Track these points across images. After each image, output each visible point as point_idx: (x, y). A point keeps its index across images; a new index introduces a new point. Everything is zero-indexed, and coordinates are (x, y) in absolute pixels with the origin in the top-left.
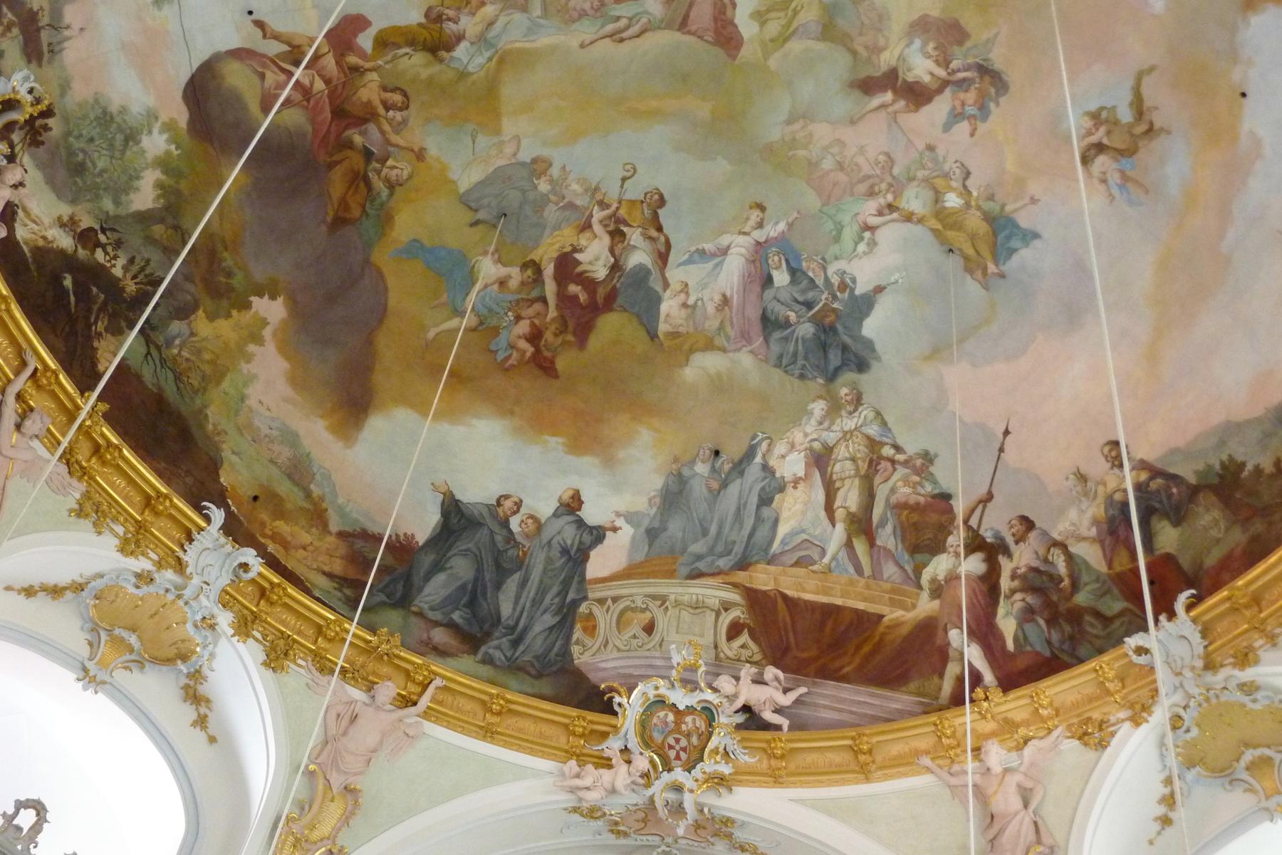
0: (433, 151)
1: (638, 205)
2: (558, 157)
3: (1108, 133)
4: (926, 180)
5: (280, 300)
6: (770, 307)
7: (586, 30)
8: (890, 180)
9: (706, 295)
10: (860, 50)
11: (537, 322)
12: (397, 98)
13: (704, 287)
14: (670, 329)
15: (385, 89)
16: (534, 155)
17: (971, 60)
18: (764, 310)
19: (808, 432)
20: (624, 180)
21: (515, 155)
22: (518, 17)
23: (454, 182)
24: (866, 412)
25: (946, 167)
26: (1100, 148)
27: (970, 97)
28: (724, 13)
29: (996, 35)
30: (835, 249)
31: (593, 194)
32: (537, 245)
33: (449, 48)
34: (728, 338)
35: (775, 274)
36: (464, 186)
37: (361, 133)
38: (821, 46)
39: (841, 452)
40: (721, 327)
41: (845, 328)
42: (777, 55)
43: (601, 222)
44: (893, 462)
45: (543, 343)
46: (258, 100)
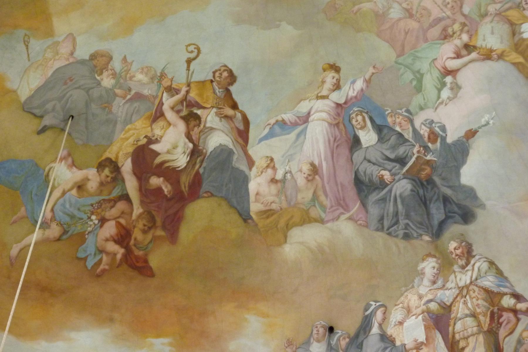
1: (208, 84)
2: (117, 49)
4: (498, 14)
6: (361, 169)
8: (462, 19)
11: (122, 221)
13: (290, 158)
16: (92, 51)
18: (356, 173)
19: (423, 293)
20: (189, 62)
21: (72, 54)
23: (15, 92)
24: (479, 264)
30: (418, 100)
31: (160, 82)
34: (323, 207)
36: (24, 94)
39: (460, 309)
41: (443, 179)
43: (172, 108)
44: (515, 312)
45: (132, 242)
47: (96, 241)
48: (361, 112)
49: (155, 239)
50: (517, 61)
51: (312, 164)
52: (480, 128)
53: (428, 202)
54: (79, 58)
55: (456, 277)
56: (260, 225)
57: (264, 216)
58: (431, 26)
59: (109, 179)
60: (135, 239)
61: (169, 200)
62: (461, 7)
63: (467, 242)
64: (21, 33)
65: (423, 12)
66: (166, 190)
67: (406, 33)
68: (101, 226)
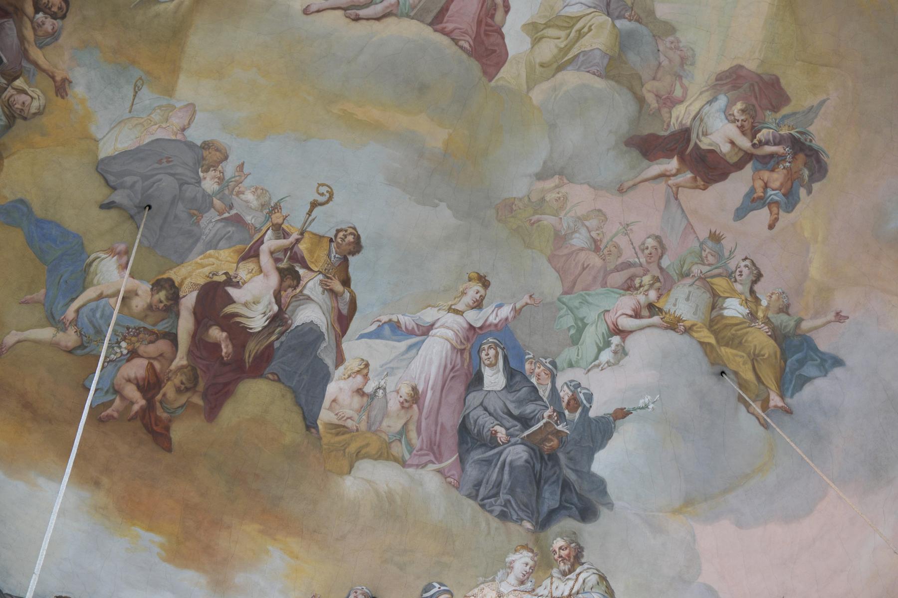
0: (79, 90)
1: (325, 243)
4: (703, 278)
6: (473, 415)
8: (657, 273)
9: (391, 384)
10: (650, 98)
11: (157, 365)
14: (334, 420)
16: (207, 139)
17: (784, 132)
20: (314, 205)
21: (183, 129)
23: (97, 141)
24: (586, 575)
25: (732, 265)
27: (777, 178)
28: (492, 17)
29: (823, 102)
30: (570, 353)
31: (270, 214)
35: (487, 373)
36: (106, 150)
38: (599, 84)
41: (571, 459)
42: (545, 85)
43: (272, 253)
45: (159, 397)
47: (115, 376)
48: (496, 345)
50: (706, 340)
51: (414, 389)
52: (634, 409)
53: (542, 482)
54: (189, 139)
55: (552, 584)
56: (325, 440)
57: (333, 431)
58: (617, 269)
59: (161, 305)
60: (164, 395)
61: (224, 364)
62: (661, 258)
63: (578, 544)
65: (613, 249)
66: (224, 350)
67: (584, 269)
68: (128, 360)
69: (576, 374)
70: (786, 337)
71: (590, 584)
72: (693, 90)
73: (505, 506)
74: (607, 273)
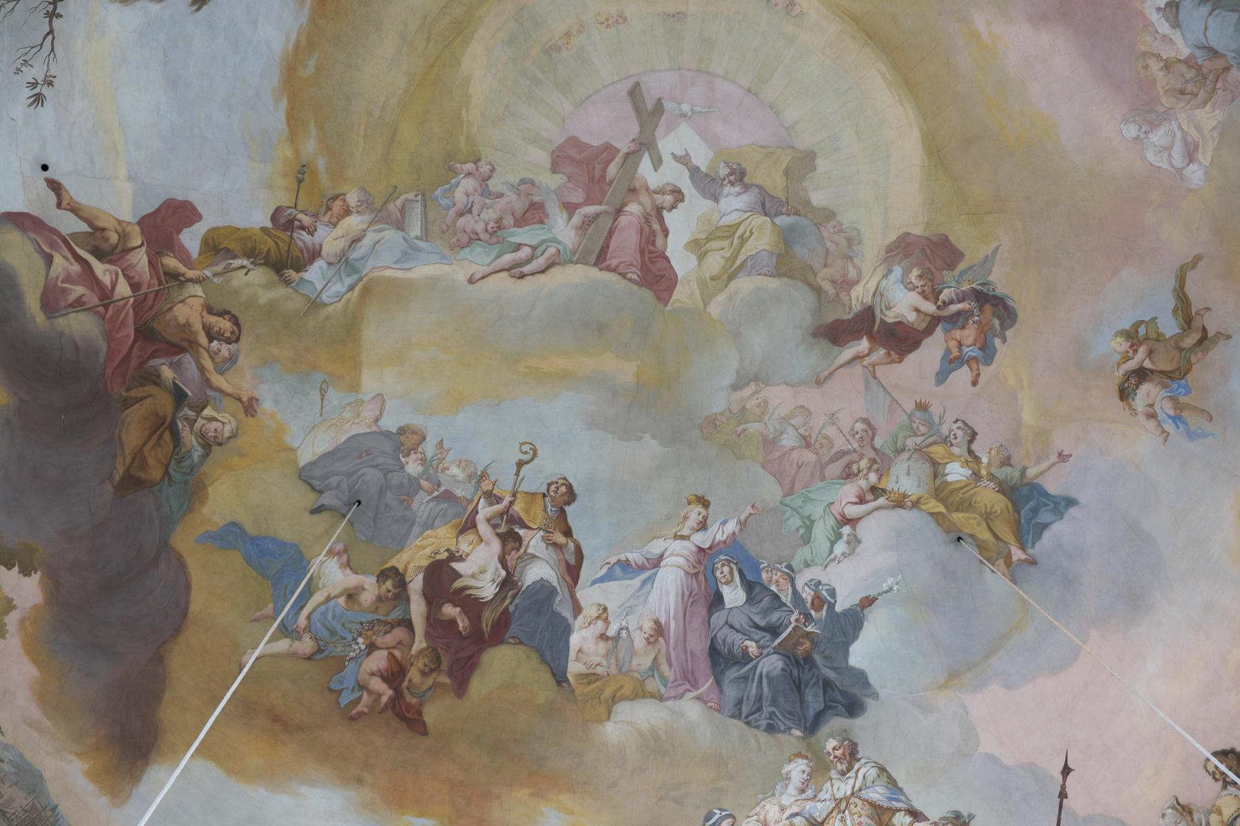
0: (267, 405)
1: (539, 499)
2: (434, 428)
3: (1150, 353)
5: (36, 577)
7: (477, 260)
8: (872, 455)
9: (632, 623)
11: (397, 654)
12: (225, 324)
13: (629, 611)
15: (210, 310)
17: (965, 287)
20: (520, 464)
21: (377, 420)
22: (390, 234)
23: (294, 450)
24: (865, 771)
25: (945, 430)
26: (1141, 374)
27: (969, 334)
28: (653, 243)
29: (996, 250)
30: (804, 553)
31: (479, 483)
32: (401, 547)
33: (299, 268)
35: (726, 591)
36: (306, 455)
37: (171, 366)
38: (773, 283)
40: (655, 664)
41: (826, 658)
42: (721, 297)
43: (488, 520)
45: (405, 684)
46: (38, 296)
47: (358, 672)
48: (729, 561)
49: (436, 686)
50: (936, 510)
51: (657, 622)
52: (879, 594)
54: (384, 429)
56: (578, 692)
58: (833, 460)
59: (390, 594)
60: (410, 681)
61: (463, 638)
62: (872, 439)
64: (319, 377)
65: (824, 441)
66: (461, 625)
67: (799, 467)
68: (368, 655)
69: (814, 573)
70: (1014, 489)
71: (870, 779)
72: (867, 267)
73: (771, 718)
74: (823, 467)
